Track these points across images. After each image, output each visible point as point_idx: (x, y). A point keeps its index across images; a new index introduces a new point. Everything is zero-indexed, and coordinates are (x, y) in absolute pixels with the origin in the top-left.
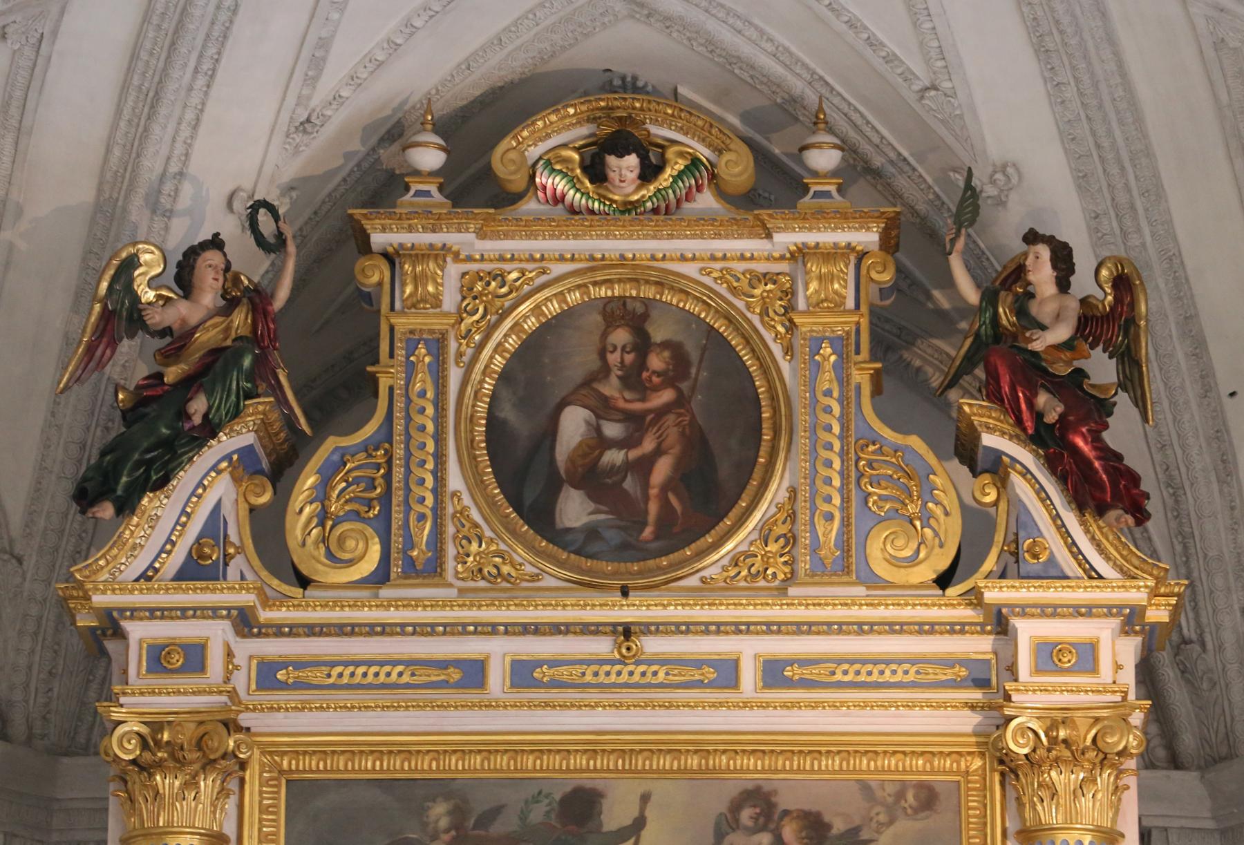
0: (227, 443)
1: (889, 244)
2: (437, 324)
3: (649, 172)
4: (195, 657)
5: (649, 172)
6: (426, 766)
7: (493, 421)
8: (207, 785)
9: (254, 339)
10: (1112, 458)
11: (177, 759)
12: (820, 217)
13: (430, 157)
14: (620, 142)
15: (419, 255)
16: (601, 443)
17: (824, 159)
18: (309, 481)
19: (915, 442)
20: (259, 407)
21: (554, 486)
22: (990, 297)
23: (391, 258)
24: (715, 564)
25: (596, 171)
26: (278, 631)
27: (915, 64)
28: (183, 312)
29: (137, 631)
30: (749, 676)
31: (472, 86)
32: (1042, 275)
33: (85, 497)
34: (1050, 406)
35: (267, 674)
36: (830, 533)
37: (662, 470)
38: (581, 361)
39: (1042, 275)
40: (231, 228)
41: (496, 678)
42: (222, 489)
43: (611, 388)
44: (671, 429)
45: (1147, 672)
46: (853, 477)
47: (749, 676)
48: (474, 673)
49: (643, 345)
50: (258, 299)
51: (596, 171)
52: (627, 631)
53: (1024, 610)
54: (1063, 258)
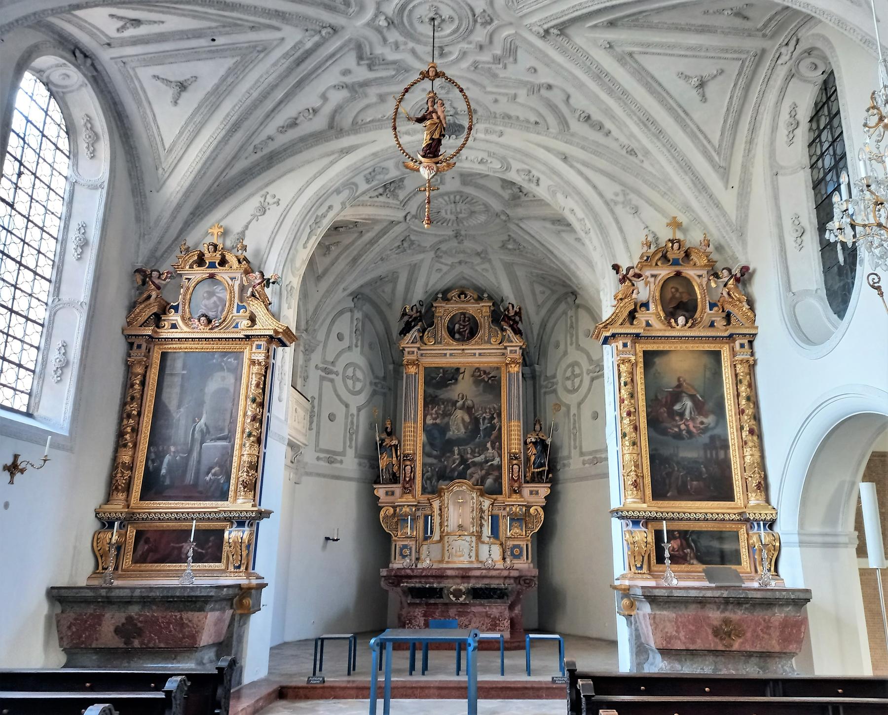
0: (416, 328)
1: (493, 305)
2: (442, 315)
3: (466, 297)
4: (413, 352)
5: (466, 297)
6: (440, 365)
7: (448, 326)
8: (415, 367)
9: (420, 316)
10: (519, 328)
11: (411, 364)
12: (485, 302)
13: (440, 296)
14: (462, 293)
15: (439, 307)
16: (460, 328)
17: (485, 295)
18: (426, 333)
19: (497, 328)
20: (420, 323)
21: (455, 334)
22: (505, 311)
23: (436, 307)
24: (473, 342)
25: (459, 297)
26: (423, 350)
27: (496, 284)
28: (412, 313)
29: (407, 350)
30: (477, 355)
31: (445, 288)
32: (511, 308)
33: (400, 334)
34: (511, 323)
35: (422, 355)
36: (486, 338)
37: (467, 332)
38: (457, 319)
39: (511, 308)
40: (418, 305)
41: (448, 355)
42: (416, 333)
43: (461, 322)
44: (468, 327)
45: (523, 354)
46: (489, 332)
47: (477, 355)
48: (445, 355)
49: (465, 317)
50: (420, 312)
51: (459, 297)
52: (463, 350)
53: (509, 346)
54: (513, 306)
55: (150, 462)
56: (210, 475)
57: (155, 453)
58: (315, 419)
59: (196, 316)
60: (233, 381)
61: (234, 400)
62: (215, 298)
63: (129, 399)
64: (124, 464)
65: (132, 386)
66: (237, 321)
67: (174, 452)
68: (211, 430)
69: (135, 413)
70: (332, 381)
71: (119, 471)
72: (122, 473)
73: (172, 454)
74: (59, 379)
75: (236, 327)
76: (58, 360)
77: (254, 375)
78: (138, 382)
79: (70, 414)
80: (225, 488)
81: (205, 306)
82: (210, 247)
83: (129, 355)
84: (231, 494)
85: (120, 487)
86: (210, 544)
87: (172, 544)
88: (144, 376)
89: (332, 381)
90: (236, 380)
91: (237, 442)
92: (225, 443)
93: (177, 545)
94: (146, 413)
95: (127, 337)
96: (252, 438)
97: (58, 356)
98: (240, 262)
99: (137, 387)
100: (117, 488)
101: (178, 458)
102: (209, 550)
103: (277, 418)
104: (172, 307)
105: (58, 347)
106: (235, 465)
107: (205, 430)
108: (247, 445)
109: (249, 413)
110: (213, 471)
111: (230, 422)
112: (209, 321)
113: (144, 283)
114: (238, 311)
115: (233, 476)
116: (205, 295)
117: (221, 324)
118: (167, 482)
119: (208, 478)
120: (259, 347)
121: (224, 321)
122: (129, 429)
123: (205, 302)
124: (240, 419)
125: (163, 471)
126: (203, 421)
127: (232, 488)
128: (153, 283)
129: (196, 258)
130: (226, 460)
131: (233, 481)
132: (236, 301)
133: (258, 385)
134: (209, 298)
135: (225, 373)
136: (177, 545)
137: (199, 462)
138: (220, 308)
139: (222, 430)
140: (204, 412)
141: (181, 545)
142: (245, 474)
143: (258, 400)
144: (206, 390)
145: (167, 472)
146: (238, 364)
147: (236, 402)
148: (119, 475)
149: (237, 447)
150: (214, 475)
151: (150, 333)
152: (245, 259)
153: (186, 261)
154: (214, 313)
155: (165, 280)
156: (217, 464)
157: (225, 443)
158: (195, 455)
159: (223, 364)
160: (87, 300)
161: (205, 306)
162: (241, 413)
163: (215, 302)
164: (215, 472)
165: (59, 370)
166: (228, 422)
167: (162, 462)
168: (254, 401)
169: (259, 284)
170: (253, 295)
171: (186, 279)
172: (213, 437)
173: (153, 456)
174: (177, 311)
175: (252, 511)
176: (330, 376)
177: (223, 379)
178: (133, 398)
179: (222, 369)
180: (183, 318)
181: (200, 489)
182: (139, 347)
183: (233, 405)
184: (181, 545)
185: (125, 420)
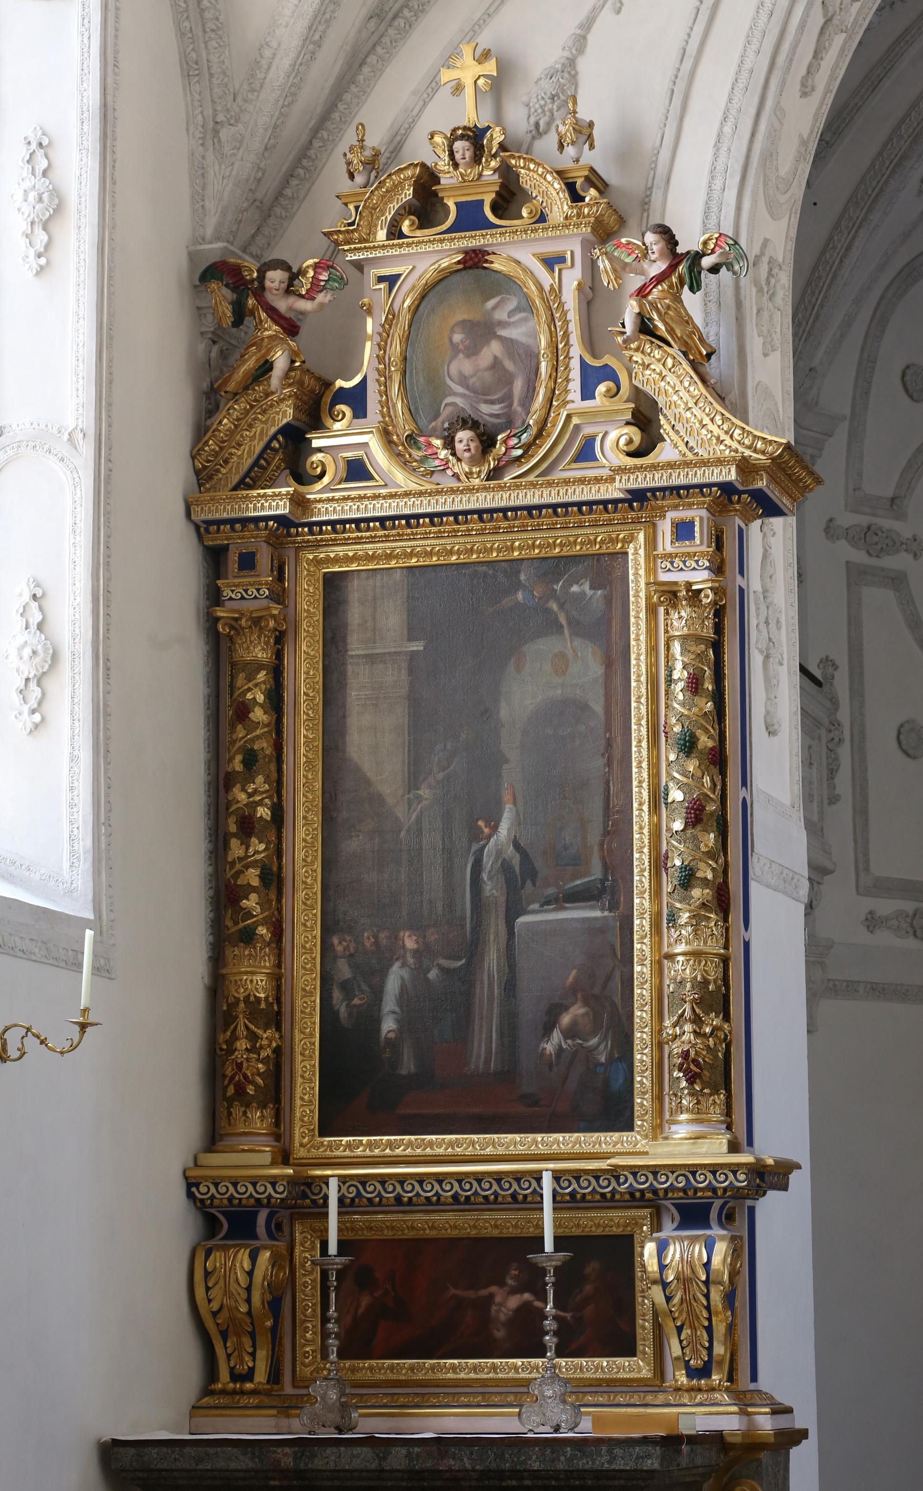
55: (337, 994)
56: (556, 1036)
58: (845, 753)
59: (441, 421)
60: (597, 669)
61: (609, 744)
62: (495, 348)
63: (238, 766)
64: (252, 1003)
65: (242, 712)
66: (588, 431)
67: (416, 953)
68: (539, 863)
69: (264, 812)
70: (897, 581)
71: (241, 1031)
72: (253, 1037)
73: (411, 960)
74: (37, 717)
75: (586, 453)
76: (27, 652)
77: (677, 647)
78: (260, 698)
79: (89, 842)
80: (618, 1082)
81: (463, 380)
82: (459, 145)
83: (214, 597)
84: (642, 1102)
85: (251, 1090)
86: (588, 1288)
87: (453, 1291)
88: (277, 671)
89: (897, 581)
90: (609, 664)
91: (641, 903)
92: (597, 914)
93: (471, 1294)
94: (301, 813)
95: (202, 529)
96: (696, 893)
97: (24, 637)
98: (576, 197)
99: (258, 715)
100: (240, 1091)
101: (433, 974)
102: (589, 1310)
103: (769, 799)
104: (342, 396)
105: (18, 605)
106: (642, 992)
107: (516, 861)
108: (684, 917)
109: (676, 795)
110: (566, 1019)
111: (606, 833)
112: (487, 442)
113: (240, 314)
114: (587, 393)
115: (642, 1036)
116: (457, 337)
117: (528, 448)
118: (408, 1065)
119: (549, 1047)
120: (683, 531)
121: (539, 435)
122: (252, 877)
123: (462, 365)
124: (641, 816)
125: (388, 1025)
126: (504, 829)
127: (642, 1080)
128: (273, 313)
129: (408, 193)
130: (609, 978)
131: (642, 1057)
132: (577, 350)
133: (694, 685)
134: (472, 351)
135: (566, 643)
136: (471, 1294)
137: (510, 987)
138: (518, 386)
139: (578, 862)
140: (507, 797)
141: (483, 1292)
142: (688, 1027)
143: (705, 742)
144: (504, 713)
145: (400, 1031)
146: (608, 600)
147: (617, 753)
148: (242, 1044)
149: (641, 924)
150: (570, 1033)
151: (283, 508)
152: (594, 180)
153: (372, 212)
154: (496, 409)
155: (309, 296)
156: (574, 990)
157: (597, 914)
158: (492, 959)
159: (555, 607)
160: (88, 420)
161: (463, 380)
162: (640, 793)
163: (496, 364)
164: (574, 1023)
165: (33, 685)
166: (594, 836)
167: (378, 994)
168: (688, 745)
169: (660, 279)
170: (645, 328)
171: (381, 279)
172: (551, 891)
173: (344, 971)
174: (360, 411)
175: (734, 1169)
176: (892, 562)
177: (561, 664)
178: (251, 759)
179: (552, 626)
180: (386, 435)
182: (248, 562)
183: (609, 764)
184: (483, 1292)
185: (234, 843)
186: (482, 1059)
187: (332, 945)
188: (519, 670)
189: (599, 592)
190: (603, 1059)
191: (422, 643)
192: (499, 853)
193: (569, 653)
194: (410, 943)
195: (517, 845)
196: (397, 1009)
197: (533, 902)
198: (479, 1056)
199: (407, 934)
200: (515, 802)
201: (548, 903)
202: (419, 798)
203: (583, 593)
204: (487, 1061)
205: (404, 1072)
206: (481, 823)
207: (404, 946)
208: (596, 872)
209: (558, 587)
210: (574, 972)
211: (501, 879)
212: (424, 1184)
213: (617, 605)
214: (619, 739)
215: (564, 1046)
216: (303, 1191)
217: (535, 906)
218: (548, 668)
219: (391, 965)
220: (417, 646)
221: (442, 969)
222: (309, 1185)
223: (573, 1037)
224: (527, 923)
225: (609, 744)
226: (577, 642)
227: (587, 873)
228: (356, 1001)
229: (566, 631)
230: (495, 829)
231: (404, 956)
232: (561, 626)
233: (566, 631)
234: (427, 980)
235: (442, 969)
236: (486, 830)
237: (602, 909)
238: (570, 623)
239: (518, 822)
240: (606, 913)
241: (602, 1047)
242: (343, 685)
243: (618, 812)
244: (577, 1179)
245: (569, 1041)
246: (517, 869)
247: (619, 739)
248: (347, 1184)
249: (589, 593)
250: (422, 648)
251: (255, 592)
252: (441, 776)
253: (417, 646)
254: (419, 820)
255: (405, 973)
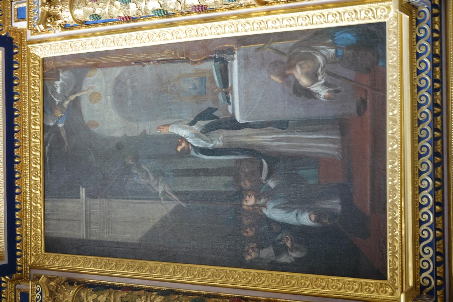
55: (284, 259)
56: (316, 88)
57: (260, 247)
60: (98, 73)
61: (138, 62)
67: (257, 198)
68: (204, 107)
73: (262, 201)
80: (350, 38)
90: (96, 66)
92: (236, 62)
101: (272, 184)
107: (202, 123)
110: (304, 81)
111: (187, 60)
126: (183, 132)
130: (277, 51)
135: (84, 95)
140: (164, 131)
144: (118, 134)
145: (310, 210)
146: (65, 68)
147: (142, 57)
150: (314, 78)
156: (284, 76)
157: (236, 62)
159: (67, 103)
164: (307, 75)
166: (188, 68)
167: (285, 226)
172: (221, 97)
179: (76, 104)
181: (351, 108)
183: (148, 61)
186: (331, 145)
187: (251, 260)
188: (97, 125)
189: (61, 74)
190: (333, 51)
191: (81, 188)
192: (197, 136)
193: (90, 91)
194: (250, 201)
195: (192, 123)
196: (295, 212)
197: (227, 110)
198: (329, 148)
199: (245, 203)
200: (168, 125)
201: (228, 99)
202: (164, 192)
203: (62, 85)
204: (332, 141)
205: (339, 208)
206: (179, 149)
207: (254, 206)
208: (210, 66)
209: (57, 101)
210: (272, 77)
211: (213, 133)
212: (422, 187)
213: (67, 63)
214: (135, 56)
215: (323, 81)
216: (427, 293)
217: (230, 108)
218: (96, 106)
219: (265, 215)
220: (83, 191)
221: (268, 177)
222: (423, 288)
223: (316, 75)
224: (241, 113)
225: (138, 62)
226: (84, 88)
227: (210, 72)
228: (289, 244)
229: (79, 95)
230: (183, 139)
231: (259, 206)
232: (77, 98)
233: (79, 95)
234: (275, 188)
235: (268, 177)
236: (184, 145)
237: (233, 59)
238: (75, 93)
239: (178, 123)
240: (235, 56)
241: (323, 52)
242: (101, 243)
243: (175, 53)
244: (418, 55)
245: (320, 78)
246: (207, 122)
247: (135, 56)
248: (422, 254)
249: (61, 81)
250: (84, 189)
251: (38, 294)
252: (151, 177)
253: (83, 191)
254: (177, 193)
255: (271, 205)
